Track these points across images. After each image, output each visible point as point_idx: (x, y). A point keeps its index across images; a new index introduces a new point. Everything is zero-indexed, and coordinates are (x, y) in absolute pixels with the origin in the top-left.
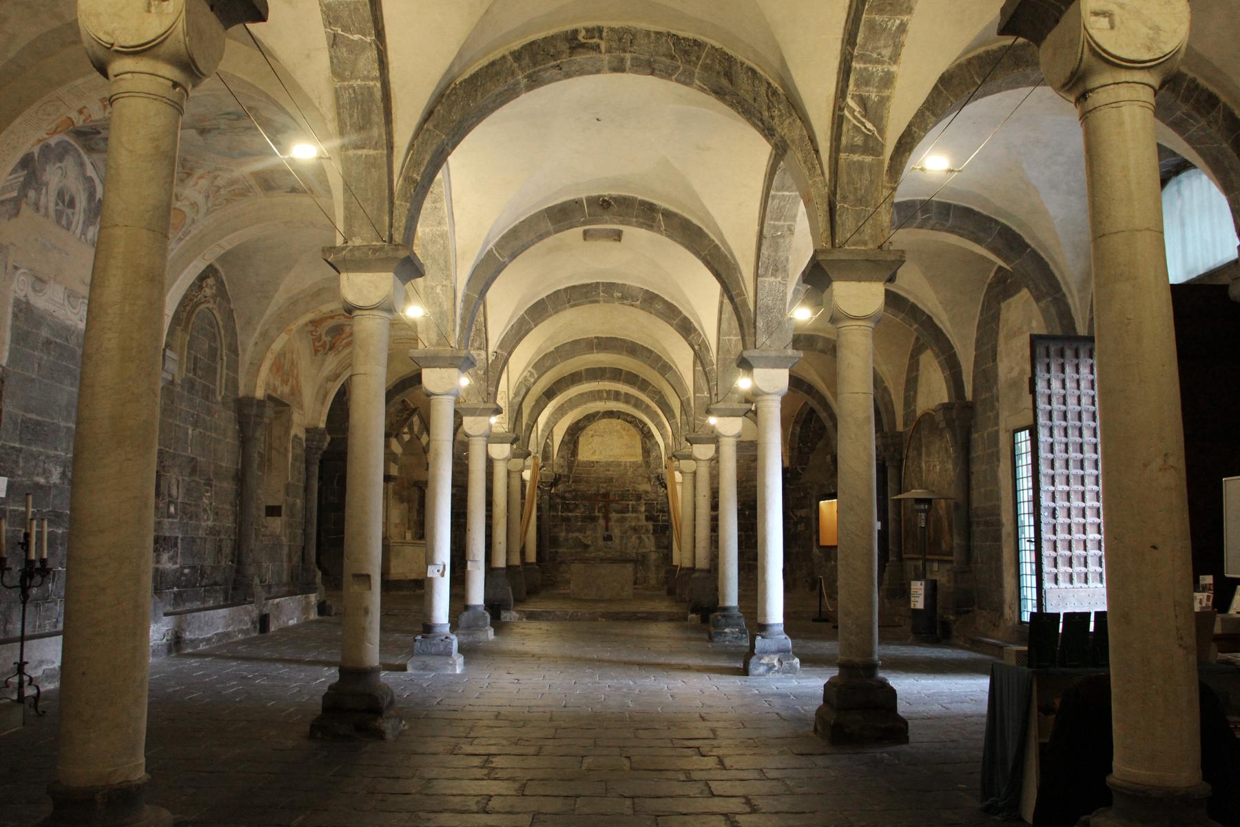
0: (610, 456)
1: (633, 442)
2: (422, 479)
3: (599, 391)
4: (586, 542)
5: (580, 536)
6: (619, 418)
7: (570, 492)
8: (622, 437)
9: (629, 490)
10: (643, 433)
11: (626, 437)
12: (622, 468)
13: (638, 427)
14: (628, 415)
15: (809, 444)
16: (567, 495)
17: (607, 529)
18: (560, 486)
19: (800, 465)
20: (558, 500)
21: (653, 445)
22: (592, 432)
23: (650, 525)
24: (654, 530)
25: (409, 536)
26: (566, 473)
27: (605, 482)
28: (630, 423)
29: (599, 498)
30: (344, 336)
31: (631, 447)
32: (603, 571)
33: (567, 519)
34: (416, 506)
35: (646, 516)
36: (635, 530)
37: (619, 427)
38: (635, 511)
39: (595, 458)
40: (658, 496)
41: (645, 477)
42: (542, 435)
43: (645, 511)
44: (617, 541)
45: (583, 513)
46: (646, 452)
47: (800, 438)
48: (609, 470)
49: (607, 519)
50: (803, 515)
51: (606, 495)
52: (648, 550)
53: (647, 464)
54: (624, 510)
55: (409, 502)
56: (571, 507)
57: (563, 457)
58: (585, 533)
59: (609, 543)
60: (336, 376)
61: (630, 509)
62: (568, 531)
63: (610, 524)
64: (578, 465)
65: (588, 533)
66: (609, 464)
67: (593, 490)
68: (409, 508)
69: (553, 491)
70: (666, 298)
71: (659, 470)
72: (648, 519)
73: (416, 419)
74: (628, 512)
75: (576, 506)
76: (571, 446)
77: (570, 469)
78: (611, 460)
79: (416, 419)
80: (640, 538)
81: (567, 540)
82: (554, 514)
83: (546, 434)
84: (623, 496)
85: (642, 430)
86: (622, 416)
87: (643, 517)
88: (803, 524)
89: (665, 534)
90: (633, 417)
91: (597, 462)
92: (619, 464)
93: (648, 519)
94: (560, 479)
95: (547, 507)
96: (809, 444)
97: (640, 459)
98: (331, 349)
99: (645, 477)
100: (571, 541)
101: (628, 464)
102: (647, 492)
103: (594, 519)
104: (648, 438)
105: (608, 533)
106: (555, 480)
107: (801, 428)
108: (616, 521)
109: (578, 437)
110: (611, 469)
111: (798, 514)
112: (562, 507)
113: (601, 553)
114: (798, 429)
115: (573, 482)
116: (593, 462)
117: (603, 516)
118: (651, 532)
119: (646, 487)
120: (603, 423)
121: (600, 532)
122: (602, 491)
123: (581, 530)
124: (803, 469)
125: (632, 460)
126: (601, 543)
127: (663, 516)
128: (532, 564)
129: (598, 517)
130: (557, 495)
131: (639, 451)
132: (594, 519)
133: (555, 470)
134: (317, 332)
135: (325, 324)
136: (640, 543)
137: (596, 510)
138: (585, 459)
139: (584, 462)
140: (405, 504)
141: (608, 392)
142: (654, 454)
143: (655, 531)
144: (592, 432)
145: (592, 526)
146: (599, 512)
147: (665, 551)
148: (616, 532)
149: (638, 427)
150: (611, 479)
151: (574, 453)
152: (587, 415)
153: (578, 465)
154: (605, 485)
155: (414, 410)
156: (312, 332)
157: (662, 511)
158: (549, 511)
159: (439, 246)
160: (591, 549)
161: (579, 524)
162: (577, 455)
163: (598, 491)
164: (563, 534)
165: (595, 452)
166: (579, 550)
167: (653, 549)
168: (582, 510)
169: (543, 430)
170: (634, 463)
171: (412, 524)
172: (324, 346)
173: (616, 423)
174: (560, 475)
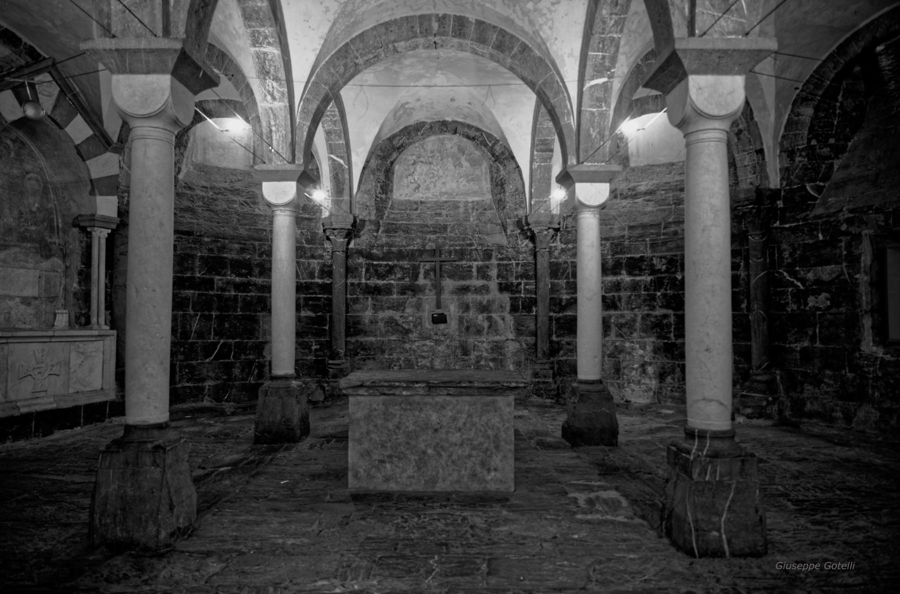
0: (442, 194)
1: (478, 172)
2: (85, 211)
3: (422, 17)
4: (407, 327)
5: (396, 315)
6: (455, 132)
7: (382, 246)
8: (461, 165)
9: (471, 245)
10: (493, 155)
11: (466, 164)
12: (461, 210)
13: (486, 145)
14: (469, 127)
15: (832, 141)
16: (375, 251)
17: (438, 306)
18: (363, 238)
19: (811, 180)
20: (361, 260)
21: (509, 173)
22: (414, 157)
23: (506, 297)
24: (512, 305)
25: (62, 319)
26: (373, 218)
27: (435, 232)
28: (473, 139)
29: (426, 257)
31: (473, 180)
32: (434, 417)
33: (376, 291)
34: (76, 263)
35: (500, 284)
36: (484, 308)
37: (455, 149)
38: (483, 273)
39: (418, 196)
40: (518, 252)
41: (497, 224)
42: (304, 111)
43: (498, 276)
44: (452, 326)
45: (400, 279)
46: (499, 185)
47: (811, 129)
48: (440, 215)
49: (439, 290)
50: (826, 277)
51: (433, 252)
52: (503, 338)
53: (500, 203)
54: (466, 274)
55: (64, 257)
56: (380, 270)
57: (367, 192)
58: (403, 311)
59: (442, 326)
61: (475, 273)
62: (375, 308)
63: (442, 297)
64: (392, 208)
65: (409, 310)
66: (440, 205)
67: (415, 246)
68: (67, 268)
69: (352, 246)
71: (521, 213)
72: (503, 288)
74: (470, 277)
75: (391, 270)
76: (382, 178)
77: (380, 210)
78: (444, 199)
80: (489, 319)
81: (373, 322)
82: (356, 281)
83: (313, 107)
84: (462, 254)
85: (492, 150)
86: (460, 129)
87: (493, 284)
88: (824, 295)
89: (530, 311)
90: (478, 130)
91: (421, 202)
92: (456, 206)
93: (503, 288)
94: (363, 226)
95: (342, 270)
96: (832, 141)
97: (488, 198)
99: (497, 224)
100: (381, 325)
101: (470, 205)
102: (500, 247)
103: (415, 290)
104: (500, 163)
105: (440, 311)
106: (354, 224)
107: (817, 109)
108: (453, 293)
109: (392, 163)
110: (444, 212)
111: (810, 276)
112: (367, 271)
113: (428, 342)
114: (808, 112)
115: (383, 232)
116: (416, 203)
117: (433, 285)
118: (508, 308)
119: (502, 240)
120: (432, 141)
121: (429, 308)
122: (430, 246)
123: (399, 306)
124: (819, 190)
125: (476, 199)
126: (428, 324)
127: (526, 284)
128: (286, 378)
129: (425, 286)
130: (360, 253)
131: (486, 185)
132: (415, 290)
133: (357, 212)
136: (489, 327)
137: (421, 276)
138: (403, 198)
139: (401, 203)
140: (56, 261)
141: (442, 19)
142: (510, 188)
143: (514, 309)
144: (414, 157)
145: (415, 299)
146: (425, 278)
147: (531, 340)
148: (452, 309)
149: (486, 145)
150: (445, 228)
151: (386, 187)
152: (406, 128)
153: (392, 208)
154: (433, 237)
157: (523, 276)
158: (347, 278)
160: (413, 336)
161: (395, 296)
162: (392, 191)
163: (424, 246)
164: (368, 314)
165: (418, 188)
166: (393, 338)
167: (511, 336)
168: (399, 276)
169: (305, 100)
170: (478, 202)
171: (71, 297)
173: (452, 142)
174: (363, 221)
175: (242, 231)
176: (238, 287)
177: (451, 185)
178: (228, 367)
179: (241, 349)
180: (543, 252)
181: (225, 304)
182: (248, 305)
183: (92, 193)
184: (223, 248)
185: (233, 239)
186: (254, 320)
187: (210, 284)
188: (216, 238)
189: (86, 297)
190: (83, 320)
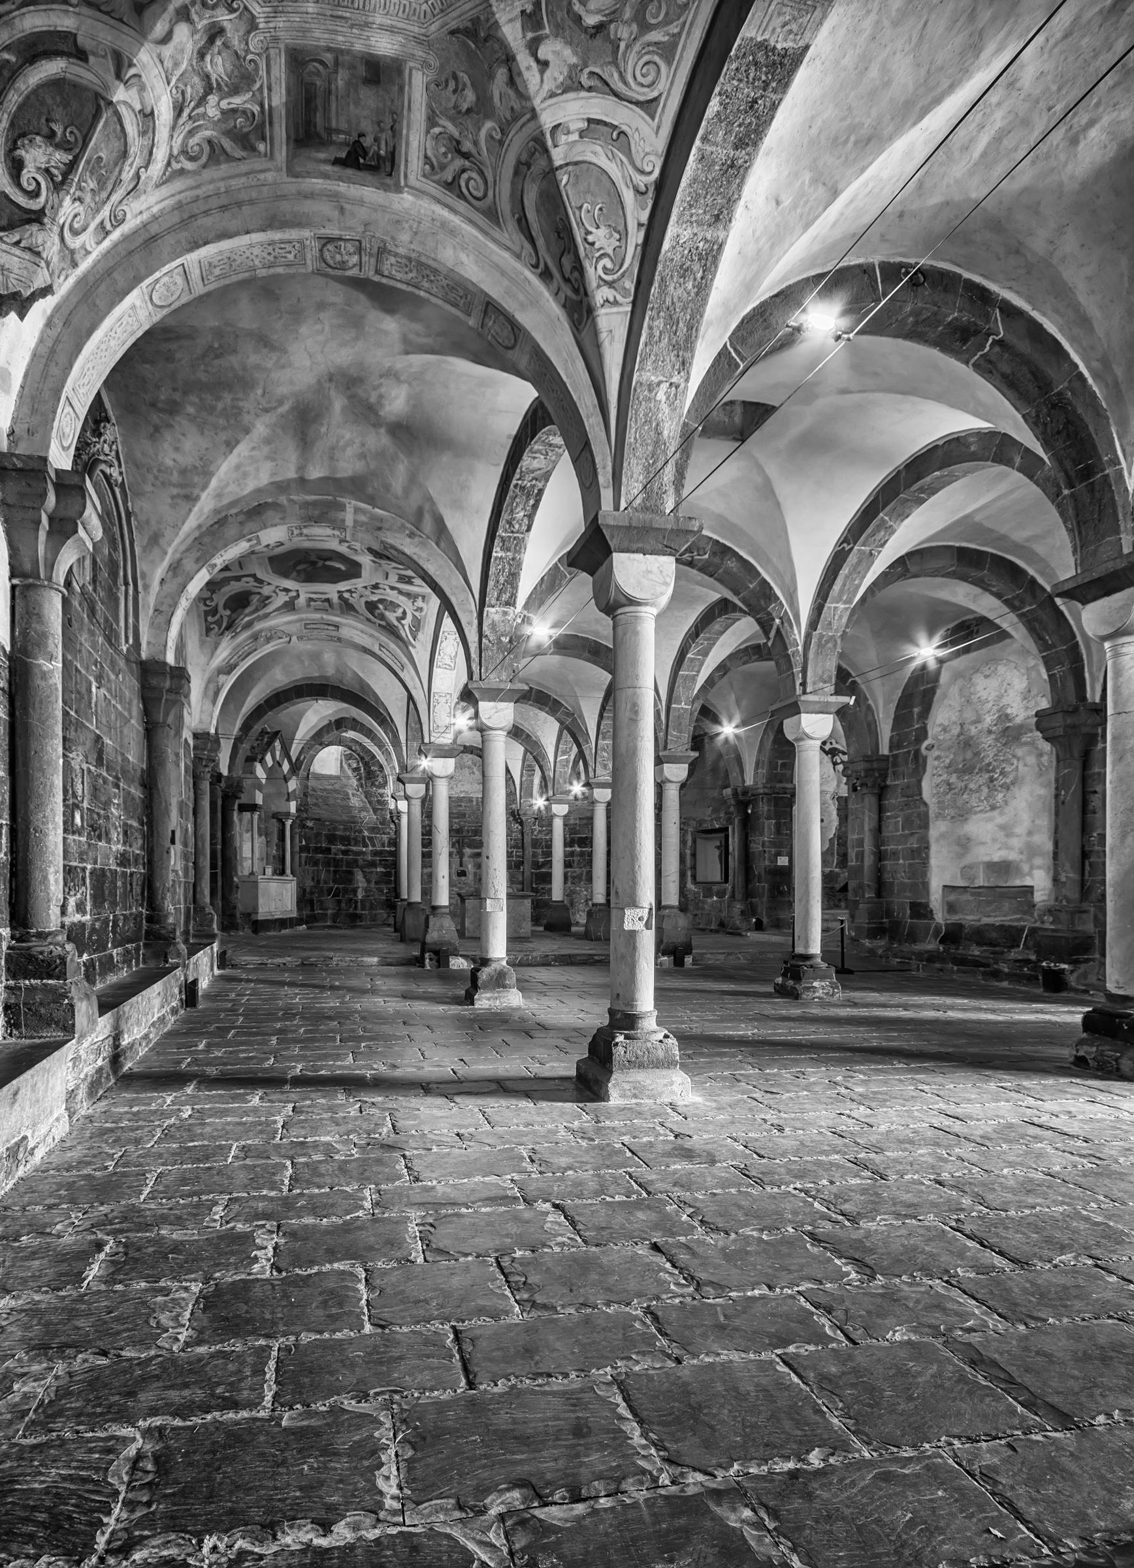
30: (247, 610)
34: (275, 840)
60: (228, 669)
70: (742, 553)
73: (277, 744)
79: (277, 744)
98: (227, 629)
134: (212, 599)
135: (226, 589)
155: (277, 733)
156: (205, 600)
159: (690, 285)
172: (219, 623)
175: (345, 818)
176: (345, 853)
177: (467, 787)
178: (339, 902)
179: (346, 891)
180: (527, 830)
181: (337, 863)
182: (349, 864)
183: (288, 800)
184: (335, 829)
185: (340, 822)
186: (351, 873)
187: (328, 850)
188: (332, 822)
189: (283, 860)
190: (283, 873)
